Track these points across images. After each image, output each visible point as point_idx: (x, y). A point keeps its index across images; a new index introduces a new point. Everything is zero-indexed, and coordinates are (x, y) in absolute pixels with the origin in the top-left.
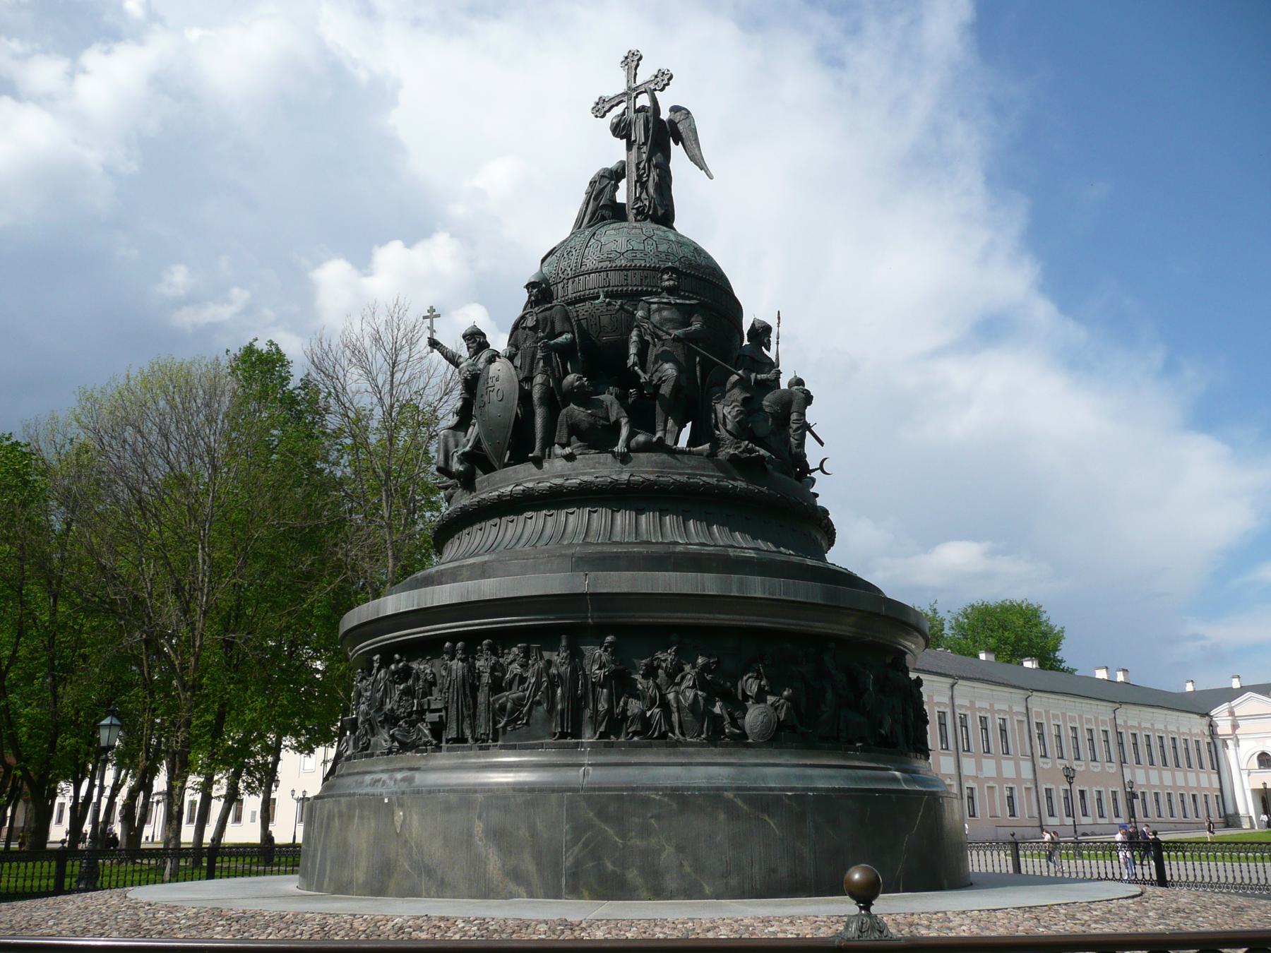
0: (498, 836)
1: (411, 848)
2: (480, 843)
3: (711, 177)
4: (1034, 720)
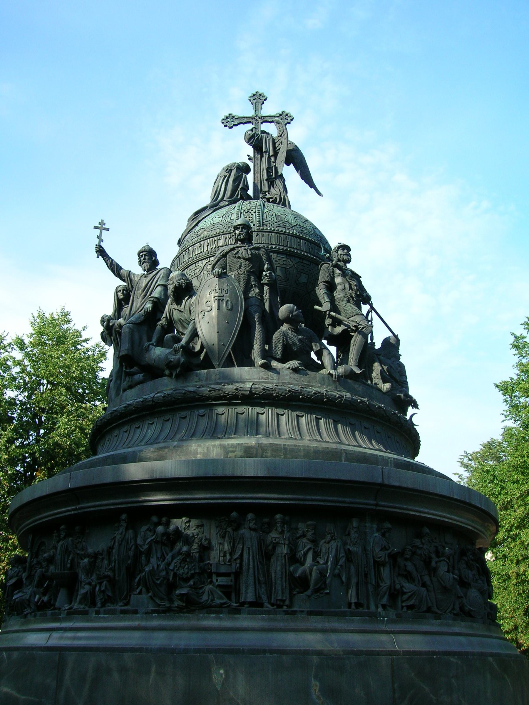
2: (318, 701)
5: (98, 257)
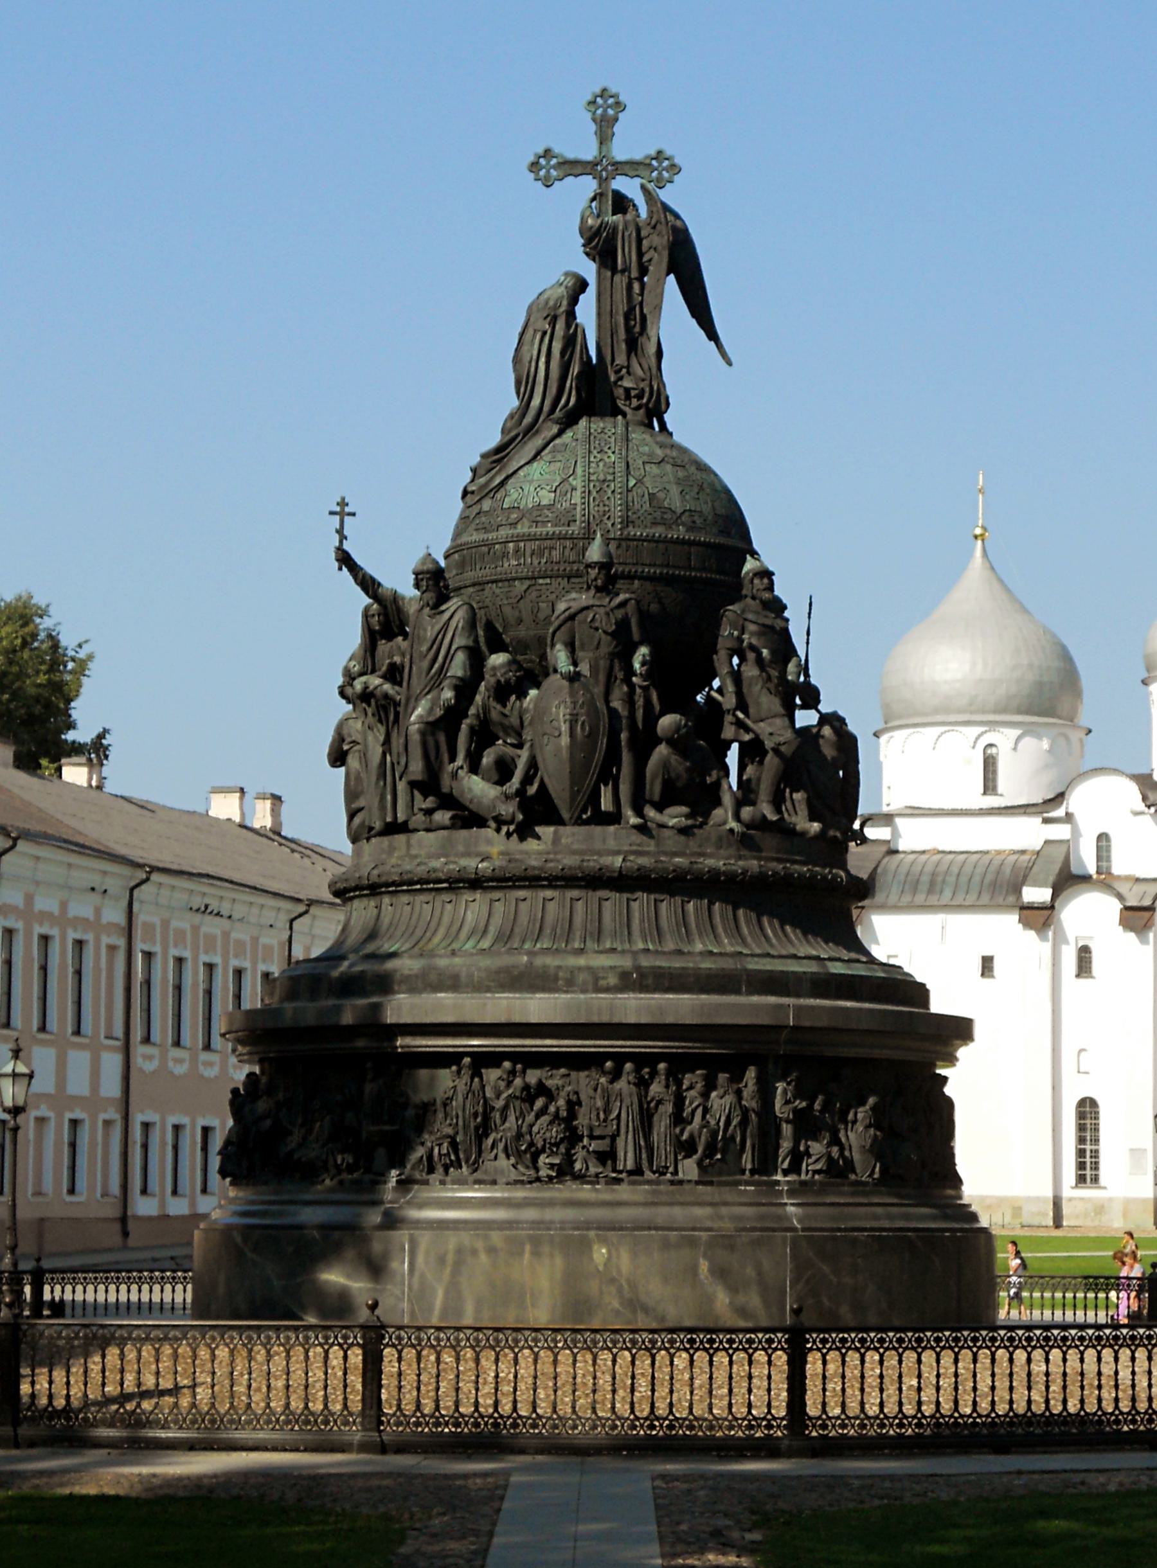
0: (721, 1273)
1: (621, 1286)
3: (729, 363)
4: (139, 946)
5: (340, 569)
